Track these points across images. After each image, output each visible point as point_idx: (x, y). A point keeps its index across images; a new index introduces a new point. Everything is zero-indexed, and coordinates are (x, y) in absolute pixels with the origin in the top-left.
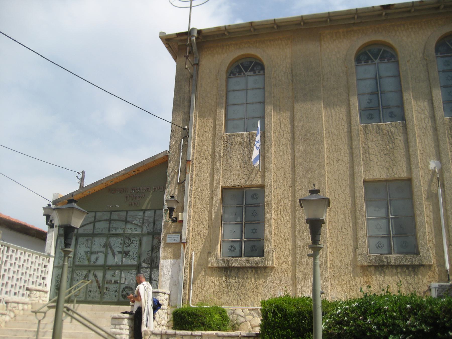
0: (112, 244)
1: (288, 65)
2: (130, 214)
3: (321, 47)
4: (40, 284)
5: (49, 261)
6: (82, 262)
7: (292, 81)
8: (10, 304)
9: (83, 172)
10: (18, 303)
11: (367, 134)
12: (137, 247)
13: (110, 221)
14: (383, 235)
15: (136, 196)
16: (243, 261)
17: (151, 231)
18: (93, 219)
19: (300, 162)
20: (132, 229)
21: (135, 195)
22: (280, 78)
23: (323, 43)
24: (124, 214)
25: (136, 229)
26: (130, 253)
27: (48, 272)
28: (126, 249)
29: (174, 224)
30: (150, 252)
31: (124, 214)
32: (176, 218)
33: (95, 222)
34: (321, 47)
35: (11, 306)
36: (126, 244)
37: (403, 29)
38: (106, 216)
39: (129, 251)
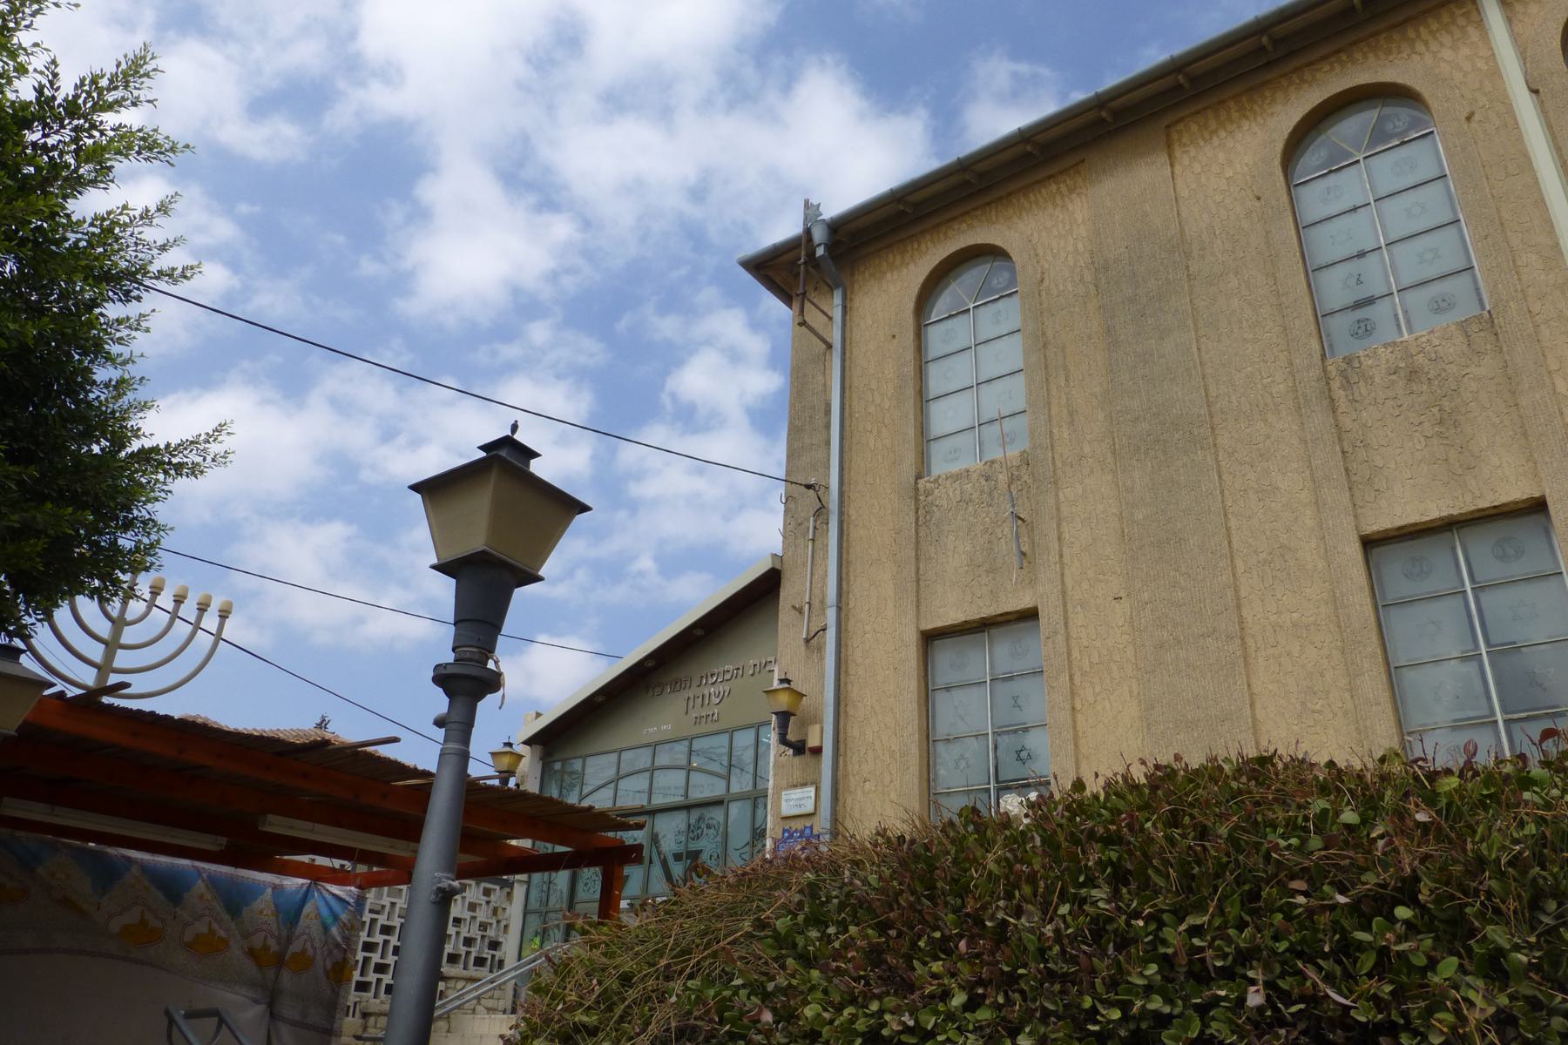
1: (1080, 246)
2: (697, 745)
3: (1172, 165)
5: (509, 895)
6: (591, 891)
7: (1096, 286)
8: (372, 1020)
11: (1355, 387)
12: (719, 839)
13: (652, 770)
14: (1455, 721)
15: (710, 694)
17: (748, 789)
18: (611, 773)
19: (1141, 517)
20: (702, 786)
21: (706, 692)
22: (1061, 288)
23: (1178, 153)
24: (682, 748)
25: (713, 785)
27: (506, 927)
28: (693, 846)
29: (797, 759)
30: (747, 849)
31: (682, 748)
32: (803, 742)
33: (619, 777)
34: (1172, 165)
35: (376, 1023)
36: (693, 832)
37: (1435, 26)
38: (643, 759)
39: (701, 851)
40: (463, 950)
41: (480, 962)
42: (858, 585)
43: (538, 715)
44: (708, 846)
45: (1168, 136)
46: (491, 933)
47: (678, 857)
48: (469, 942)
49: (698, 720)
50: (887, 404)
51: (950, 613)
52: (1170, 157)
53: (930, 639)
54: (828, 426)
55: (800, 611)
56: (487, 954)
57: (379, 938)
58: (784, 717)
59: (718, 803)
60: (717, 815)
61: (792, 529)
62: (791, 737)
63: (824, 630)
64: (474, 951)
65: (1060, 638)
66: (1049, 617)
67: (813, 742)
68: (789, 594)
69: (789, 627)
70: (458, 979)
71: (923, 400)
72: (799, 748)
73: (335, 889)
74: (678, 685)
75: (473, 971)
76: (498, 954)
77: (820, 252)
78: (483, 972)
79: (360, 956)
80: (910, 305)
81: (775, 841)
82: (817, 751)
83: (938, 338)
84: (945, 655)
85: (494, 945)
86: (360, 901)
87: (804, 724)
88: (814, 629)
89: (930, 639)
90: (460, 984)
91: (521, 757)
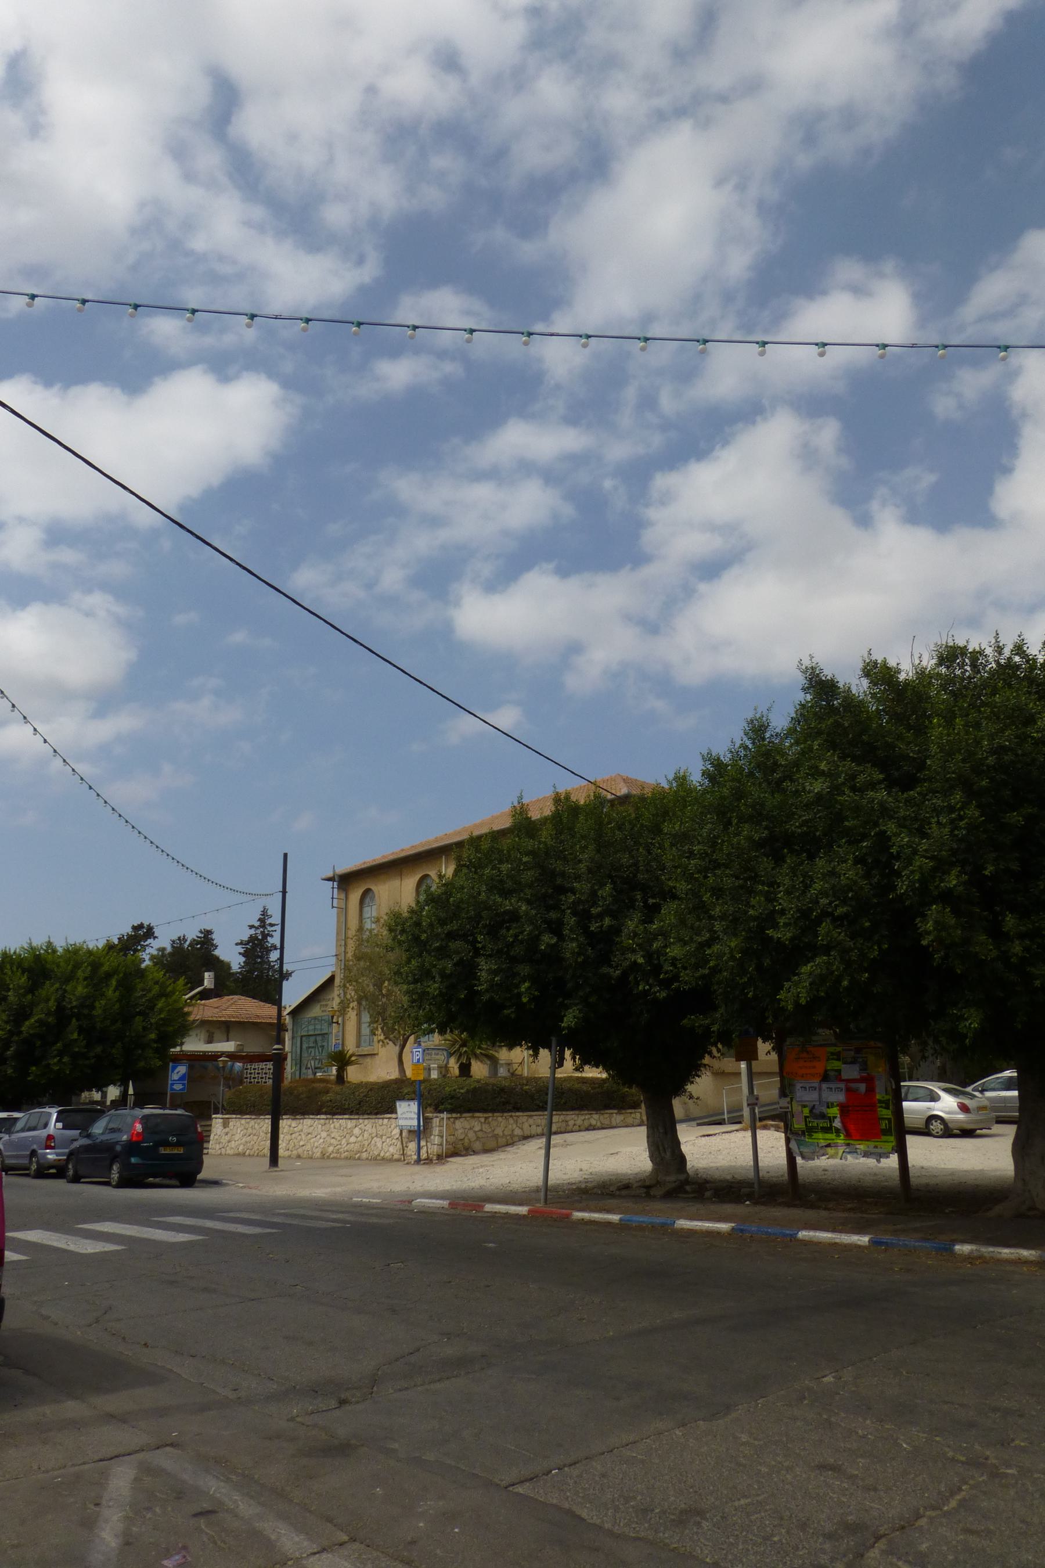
28: (323, 1044)
59: (326, 1034)
73: (239, 1064)
74: (319, 1001)
83: (366, 909)
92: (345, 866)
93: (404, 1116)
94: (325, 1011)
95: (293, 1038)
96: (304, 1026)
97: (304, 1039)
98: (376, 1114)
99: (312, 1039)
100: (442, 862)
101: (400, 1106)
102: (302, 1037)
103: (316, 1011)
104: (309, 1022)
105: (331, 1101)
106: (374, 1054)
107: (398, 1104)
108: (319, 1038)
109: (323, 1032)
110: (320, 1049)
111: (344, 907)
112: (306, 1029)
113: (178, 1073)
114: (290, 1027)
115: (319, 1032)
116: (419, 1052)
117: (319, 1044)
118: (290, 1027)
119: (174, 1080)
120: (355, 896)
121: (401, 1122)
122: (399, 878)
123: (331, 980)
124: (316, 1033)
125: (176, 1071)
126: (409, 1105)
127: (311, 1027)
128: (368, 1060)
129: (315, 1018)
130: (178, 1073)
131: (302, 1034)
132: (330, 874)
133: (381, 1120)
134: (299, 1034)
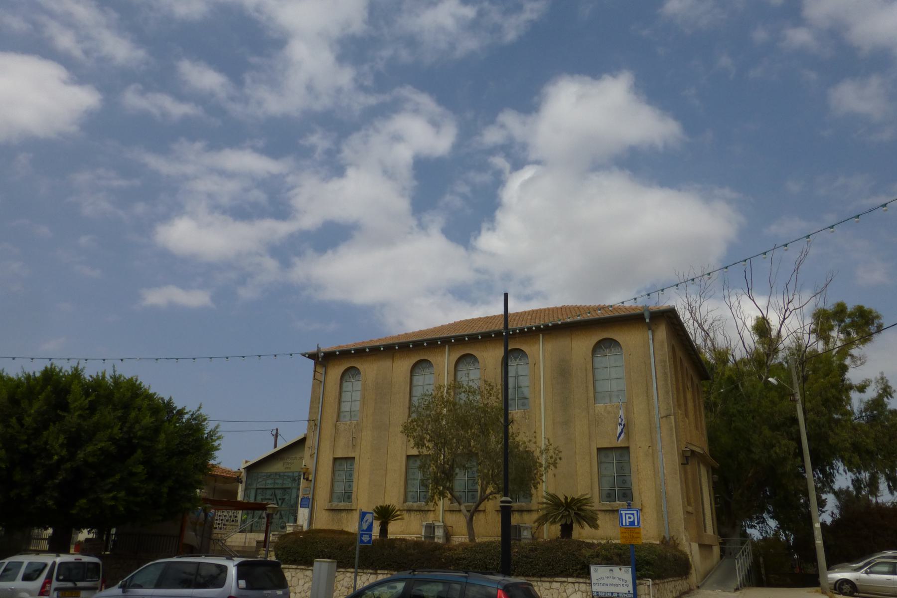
0: (276, 493)
4: (233, 521)
9: (277, 430)
10: (218, 534)
16: (343, 505)
23: (394, 360)
26: (286, 500)
28: (284, 497)
40: (229, 518)
41: (233, 521)
42: (322, 444)
43: (246, 462)
44: (287, 497)
45: (393, 357)
46: (235, 514)
47: (280, 499)
48: (230, 517)
49: (286, 468)
50: (332, 401)
51: (339, 455)
52: (393, 360)
53: (335, 459)
54: (319, 403)
55: (310, 448)
56: (234, 519)
57: (218, 518)
58: (304, 474)
59: (289, 488)
60: (288, 490)
61: (309, 428)
62: (305, 477)
63: (314, 453)
64: (232, 519)
65: (358, 465)
66: (357, 460)
67: (310, 479)
68: (308, 443)
69: (307, 453)
70: (228, 525)
71: (340, 402)
72: (307, 479)
75: (231, 523)
76: (237, 519)
77: (320, 359)
78: (233, 523)
79: (215, 522)
80: (339, 377)
81: (301, 499)
82: (311, 481)
83: (345, 384)
84: (338, 463)
85: (236, 517)
86: (215, 513)
87: (309, 474)
88: (313, 453)
89: (335, 459)
90: (229, 526)
91: (242, 472)
92: (326, 347)
93: (602, 582)
94: (290, 468)
95: (246, 490)
96: (260, 480)
97: (259, 491)
98: (541, 576)
99: (269, 492)
100: (445, 351)
101: (596, 571)
102: (257, 489)
103: (278, 467)
104: (269, 476)
105: (464, 559)
106: (352, 510)
107: (592, 568)
108: (278, 492)
109: (285, 486)
110: (280, 503)
111: (323, 380)
112: (264, 482)
113: (366, 521)
114: (244, 480)
115: (280, 486)
116: (633, 514)
117: (278, 497)
118: (244, 480)
119: (363, 531)
120: (335, 372)
121: (595, 588)
122: (391, 361)
123: (302, 442)
124: (276, 486)
125: (364, 520)
126: (611, 570)
127: (269, 481)
128: (344, 514)
129: (276, 473)
130: (366, 521)
131: (258, 486)
132: (313, 350)
133: (548, 583)
134: (254, 486)
